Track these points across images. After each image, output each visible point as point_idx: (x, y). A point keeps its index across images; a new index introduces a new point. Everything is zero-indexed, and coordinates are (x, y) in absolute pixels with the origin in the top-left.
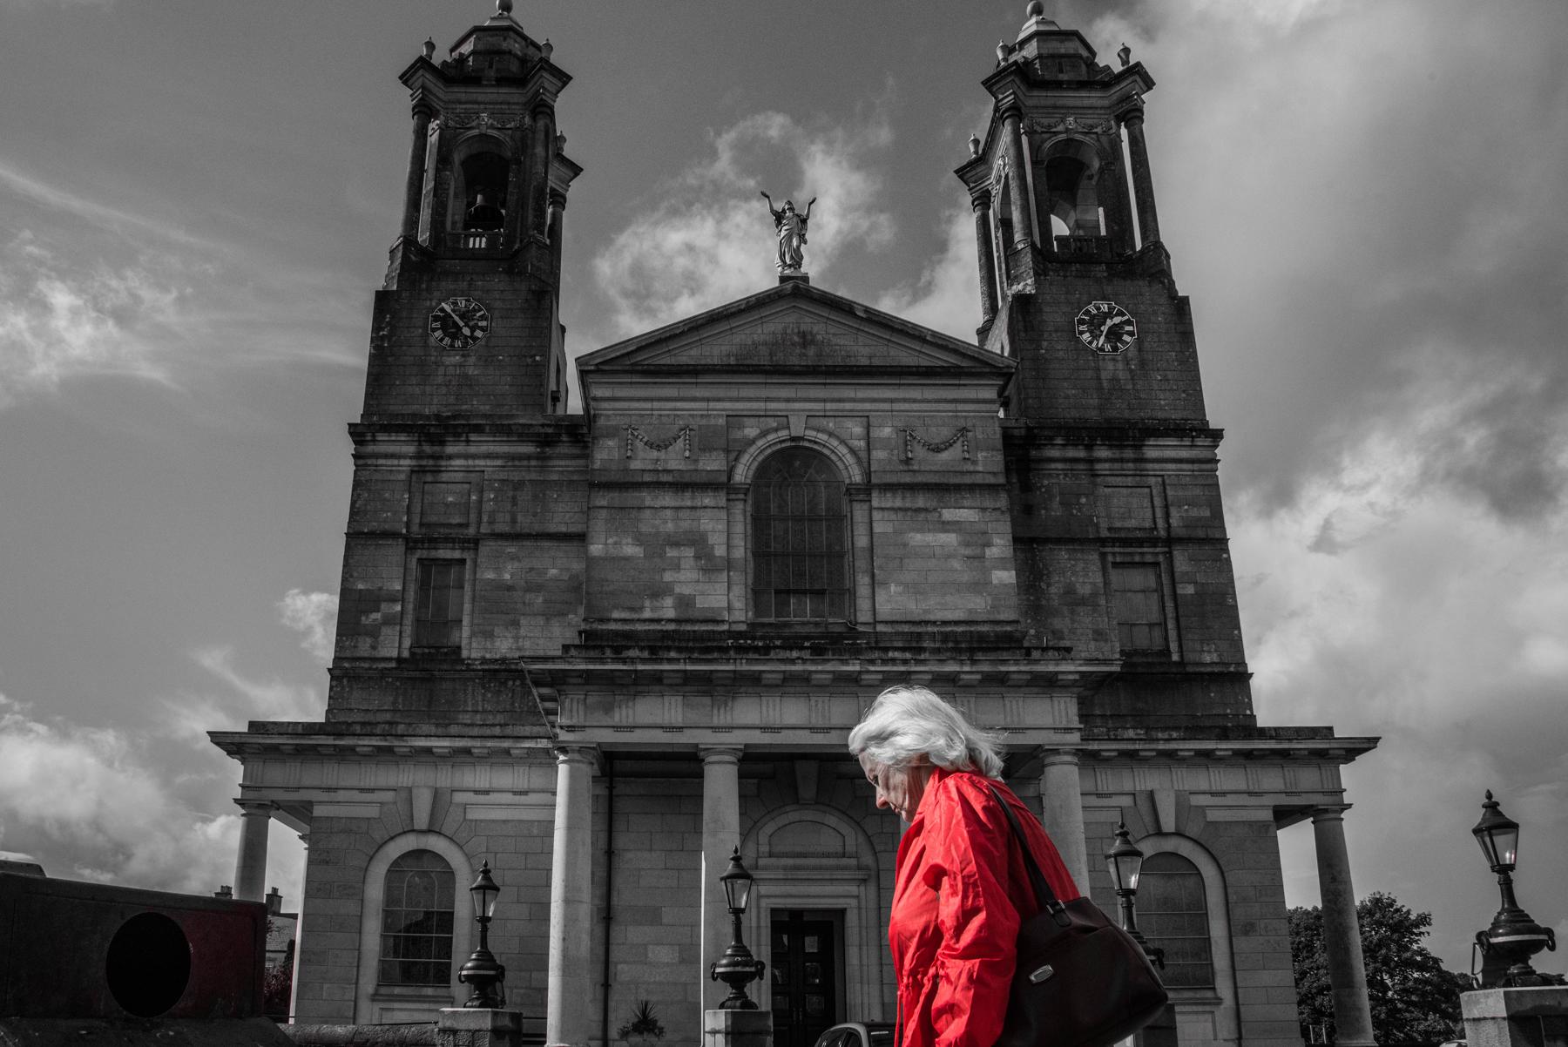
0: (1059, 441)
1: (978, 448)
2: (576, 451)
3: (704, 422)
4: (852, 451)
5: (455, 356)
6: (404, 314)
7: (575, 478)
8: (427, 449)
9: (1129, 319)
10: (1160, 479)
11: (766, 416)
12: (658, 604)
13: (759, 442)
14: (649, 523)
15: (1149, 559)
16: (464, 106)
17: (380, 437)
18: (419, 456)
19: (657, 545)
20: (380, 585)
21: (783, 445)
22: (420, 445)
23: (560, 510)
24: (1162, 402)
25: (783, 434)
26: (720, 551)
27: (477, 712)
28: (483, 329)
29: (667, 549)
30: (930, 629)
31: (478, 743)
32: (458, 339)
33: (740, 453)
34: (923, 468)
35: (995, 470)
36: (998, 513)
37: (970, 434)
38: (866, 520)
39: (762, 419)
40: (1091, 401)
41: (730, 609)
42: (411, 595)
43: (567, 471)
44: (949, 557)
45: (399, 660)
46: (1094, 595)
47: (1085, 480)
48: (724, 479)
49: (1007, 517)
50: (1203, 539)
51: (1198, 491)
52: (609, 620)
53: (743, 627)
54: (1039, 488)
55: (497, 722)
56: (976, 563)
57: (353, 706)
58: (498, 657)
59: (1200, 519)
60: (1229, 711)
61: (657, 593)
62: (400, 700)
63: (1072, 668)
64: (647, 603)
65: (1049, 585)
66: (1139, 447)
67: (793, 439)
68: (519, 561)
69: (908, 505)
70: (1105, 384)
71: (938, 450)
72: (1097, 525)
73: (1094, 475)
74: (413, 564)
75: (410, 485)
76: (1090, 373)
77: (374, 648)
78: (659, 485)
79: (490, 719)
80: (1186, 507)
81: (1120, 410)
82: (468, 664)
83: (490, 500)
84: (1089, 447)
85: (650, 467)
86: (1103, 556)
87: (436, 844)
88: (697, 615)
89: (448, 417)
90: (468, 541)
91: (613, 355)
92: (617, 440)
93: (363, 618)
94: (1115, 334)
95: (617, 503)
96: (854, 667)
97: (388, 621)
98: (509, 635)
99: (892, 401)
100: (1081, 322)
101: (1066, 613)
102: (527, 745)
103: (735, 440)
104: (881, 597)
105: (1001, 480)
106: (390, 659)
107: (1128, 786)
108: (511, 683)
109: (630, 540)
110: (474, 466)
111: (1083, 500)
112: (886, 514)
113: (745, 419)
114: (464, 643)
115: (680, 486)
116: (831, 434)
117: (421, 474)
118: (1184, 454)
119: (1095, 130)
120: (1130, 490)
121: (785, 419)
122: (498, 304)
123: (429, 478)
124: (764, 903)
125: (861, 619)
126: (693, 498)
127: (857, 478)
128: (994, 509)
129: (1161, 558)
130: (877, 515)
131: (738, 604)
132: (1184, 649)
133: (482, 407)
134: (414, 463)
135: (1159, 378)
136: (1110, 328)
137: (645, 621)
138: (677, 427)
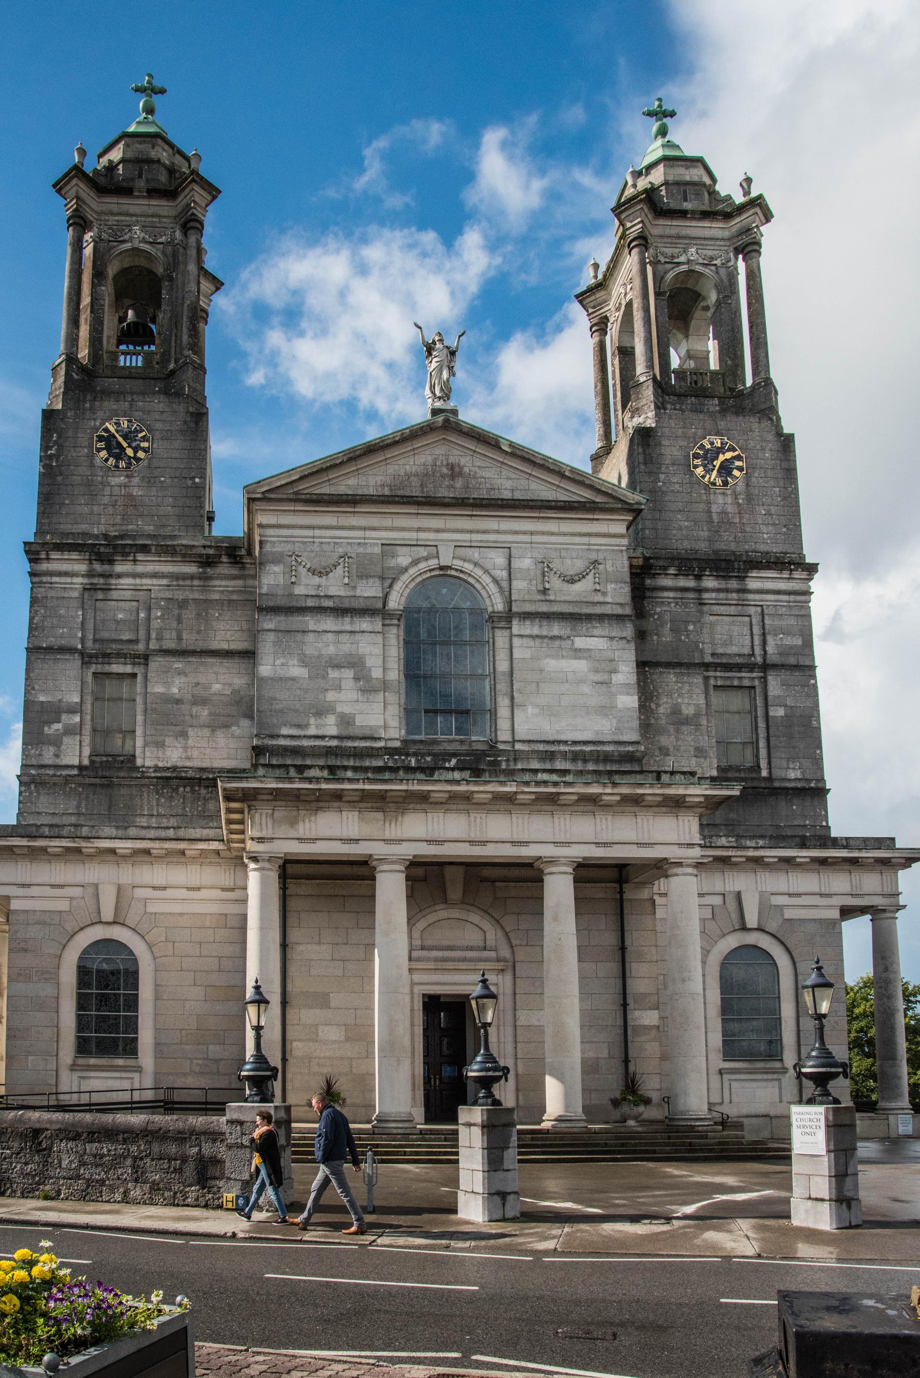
0: (672, 571)
2: (235, 572)
7: (235, 597)
8: (97, 567)
10: (759, 609)
12: (323, 722)
14: (312, 646)
17: (54, 555)
18: (90, 574)
22: (91, 563)
23: (222, 628)
26: (377, 673)
27: (153, 815)
28: (145, 450)
30: (563, 748)
31: (157, 844)
33: (394, 580)
34: (558, 599)
35: (623, 602)
36: (624, 641)
37: (601, 567)
38: (507, 646)
40: (702, 533)
41: (385, 727)
42: (88, 707)
44: (581, 681)
49: (632, 646)
52: (278, 736)
53: (397, 744)
55: (170, 825)
56: (603, 687)
58: (169, 765)
61: (321, 712)
62: (83, 805)
63: (698, 792)
64: (312, 721)
66: (742, 578)
67: (442, 568)
68: (186, 676)
69: (545, 633)
71: (572, 581)
74: (89, 678)
75: (83, 602)
79: (165, 822)
81: (727, 543)
82: (143, 772)
83: (157, 618)
84: (698, 577)
85: (314, 593)
88: (359, 733)
89: (116, 537)
92: (282, 566)
96: (511, 788)
98: (178, 745)
102: (200, 847)
103: (389, 568)
104: (519, 716)
105: (628, 611)
106: (72, 767)
108: (181, 789)
109: (295, 662)
110: (141, 585)
112: (525, 640)
114: (138, 752)
117: (93, 591)
118: (782, 586)
120: (732, 618)
121: (434, 548)
123: (100, 595)
124: (418, 990)
125: (500, 738)
126: (351, 623)
127: (500, 606)
128: (621, 638)
130: (516, 642)
131: (394, 722)
134: (86, 581)
137: (310, 737)
138: (336, 555)
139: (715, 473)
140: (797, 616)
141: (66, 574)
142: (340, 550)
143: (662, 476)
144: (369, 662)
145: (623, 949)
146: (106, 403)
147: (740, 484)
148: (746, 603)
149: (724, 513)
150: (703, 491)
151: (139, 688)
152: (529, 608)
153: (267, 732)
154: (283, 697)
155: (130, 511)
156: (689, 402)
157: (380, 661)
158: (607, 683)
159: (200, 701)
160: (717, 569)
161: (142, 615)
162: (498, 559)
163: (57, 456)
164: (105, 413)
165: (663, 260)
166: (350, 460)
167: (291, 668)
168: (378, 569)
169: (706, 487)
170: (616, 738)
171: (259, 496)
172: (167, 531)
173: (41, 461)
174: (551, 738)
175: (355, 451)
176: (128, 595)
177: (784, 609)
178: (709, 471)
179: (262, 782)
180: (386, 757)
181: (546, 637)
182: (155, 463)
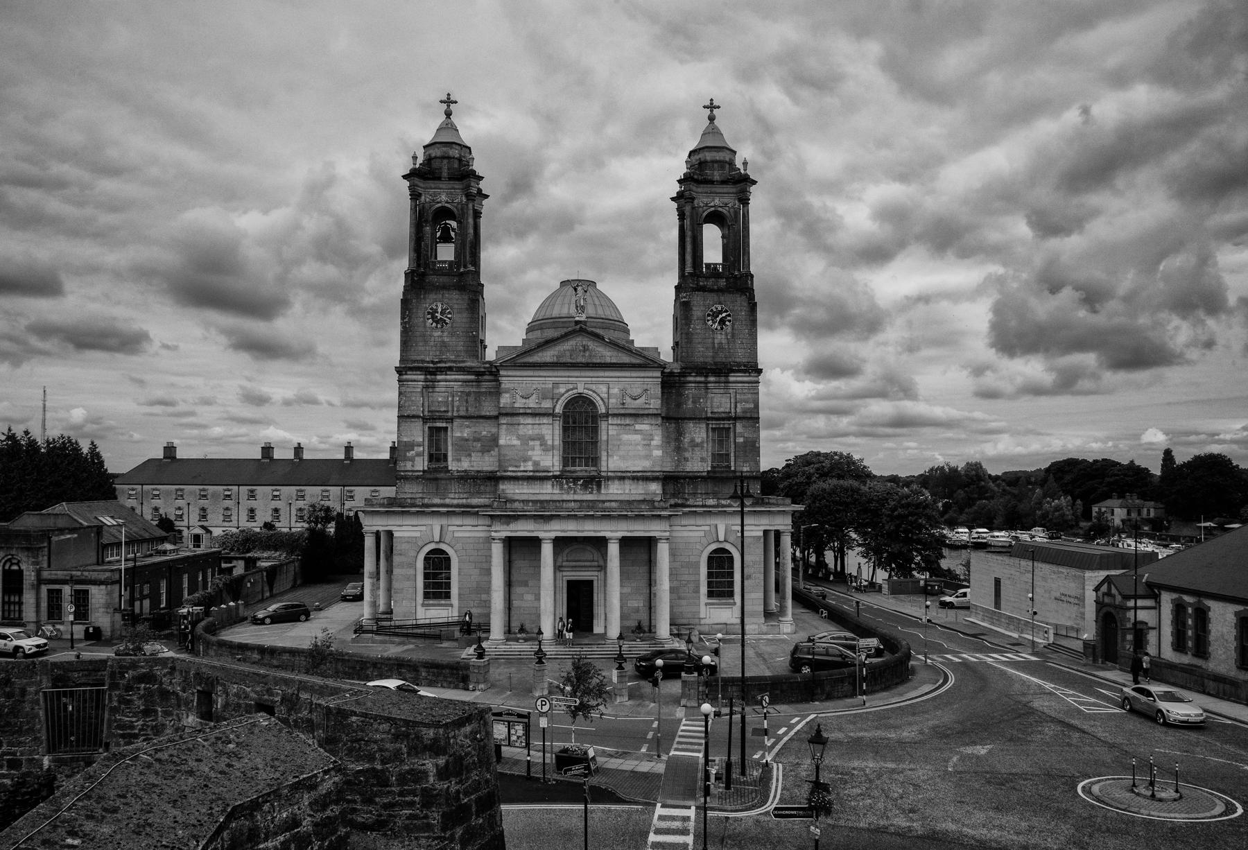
3: (544, 386)
4: (602, 399)
8: (429, 377)
14: (522, 430)
15: (727, 426)
18: (426, 381)
19: (525, 440)
25: (575, 391)
26: (550, 442)
30: (629, 474)
33: (558, 399)
42: (426, 443)
45: (424, 471)
46: (702, 442)
47: (703, 391)
48: (551, 412)
51: (750, 396)
53: (558, 473)
59: (749, 409)
61: (525, 461)
64: (522, 464)
70: (716, 345)
72: (706, 412)
74: (426, 429)
77: (413, 466)
79: (462, 496)
81: (721, 358)
86: (708, 425)
87: (443, 547)
88: (542, 469)
89: (437, 362)
94: (722, 322)
95: (510, 422)
97: (418, 455)
100: (709, 315)
106: (420, 471)
107: (708, 523)
115: (534, 415)
116: (594, 392)
122: (456, 306)
129: (731, 426)
131: (557, 463)
141: (415, 381)
143: (692, 326)
145: (650, 561)
151: (449, 433)
152: (616, 412)
154: (510, 454)
155: (443, 349)
158: (649, 445)
159: (477, 440)
162: (603, 389)
163: (408, 322)
166: (538, 347)
176: (443, 389)
178: (714, 323)
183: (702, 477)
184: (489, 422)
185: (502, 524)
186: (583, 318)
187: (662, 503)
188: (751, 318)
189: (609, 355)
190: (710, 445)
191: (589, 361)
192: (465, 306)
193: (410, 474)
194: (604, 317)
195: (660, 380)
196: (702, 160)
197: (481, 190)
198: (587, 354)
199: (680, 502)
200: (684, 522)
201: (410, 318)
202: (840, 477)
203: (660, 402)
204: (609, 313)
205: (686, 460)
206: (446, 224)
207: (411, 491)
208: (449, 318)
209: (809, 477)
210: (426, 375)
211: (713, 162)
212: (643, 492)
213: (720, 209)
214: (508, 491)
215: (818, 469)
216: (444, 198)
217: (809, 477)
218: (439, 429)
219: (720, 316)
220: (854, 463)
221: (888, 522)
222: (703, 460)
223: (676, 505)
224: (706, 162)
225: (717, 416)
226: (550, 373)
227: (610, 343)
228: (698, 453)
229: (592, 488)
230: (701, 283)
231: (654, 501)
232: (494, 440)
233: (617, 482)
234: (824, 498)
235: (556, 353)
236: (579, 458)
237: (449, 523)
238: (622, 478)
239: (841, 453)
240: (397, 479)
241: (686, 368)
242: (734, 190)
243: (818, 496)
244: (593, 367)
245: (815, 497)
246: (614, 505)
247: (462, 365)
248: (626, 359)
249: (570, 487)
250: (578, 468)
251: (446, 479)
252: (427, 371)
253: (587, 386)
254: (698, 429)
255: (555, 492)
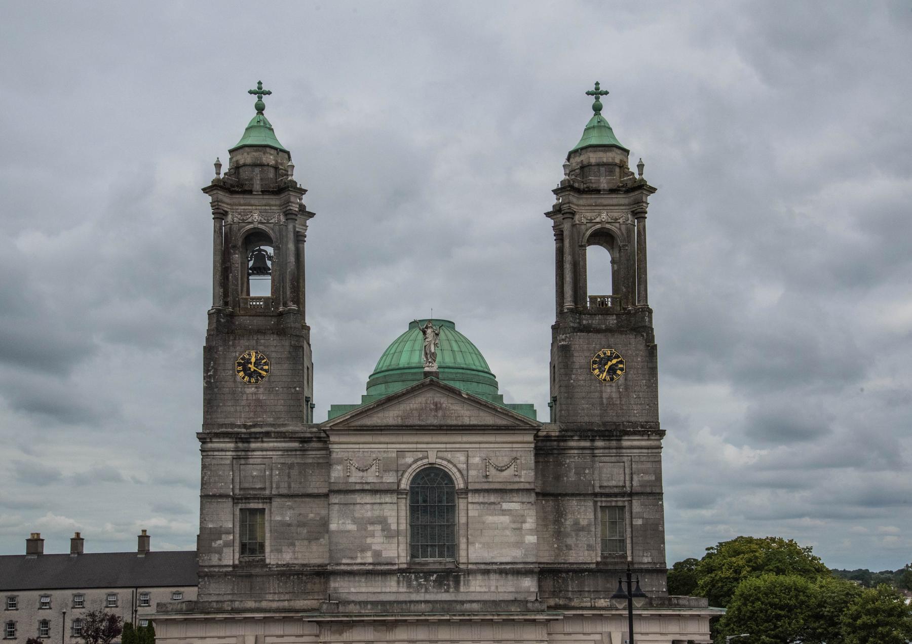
1: (522, 469)
3: (385, 455)
4: (459, 471)
5: (251, 388)
6: (221, 361)
7: (321, 461)
8: (240, 445)
9: (621, 360)
10: (630, 458)
11: (416, 451)
13: (412, 464)
14: (359, 512)
15: (620, 504)
16: (243, 207)
18: (236, 450)
19: (363, 524)
20: (221, 525)
21: (426, 467)
23: (314, 480)
24: (635, 412)
25: (425, 461)
26: (394, 527)
29: (368, 526)
30: (495, 567)
32: (252, 377)
33: (404, 472)
34: (494, 481)
36: (530, 505)
37: (518, 461)
38: (466, 508)
39: (415, 453)
40: (596, 411)
41: (398, 557)
43: (316, 457)
45: (234, 566)
46: (589, 525)
47: (588, 459)
48: (396, 487)
50: (650, 493)
51: (649, 465)
52: (341, 564)
53: (405, 566)
54: (564, 465)
55: (286, 599)
56: (518, 532)
57: (211, 592)
58: (285, 563)
60: (654, 589)
61: (363, 551)
62: (236, 589)
64: (359, 555)
65: (566, 520)
68: (294, 509)
69: (486, 501)
70: (605, 401)
72: (593, 486)
73: (594, 456)
74: (238, 512)
75: (233, 466)
76: (597, 394)
78: (363, 491)
80: (642, 475)
82: (270, 568)
83: (276, 475)
85: (359, 481)
86: (595, 502)
88: (383, 560)
89: (251, 427)
90: (266, 498)
91: (339, 421)
92: (342, 465)
93: (213, 544)
94: (612, 370)
95: (343, 501)
97: (227, 545)
98: (290, 551)
99: (480, 443)
100: (595, 362)
101: (574, 535)
107: (599, 629)
108: (292, 577)
109: (350, 522)
110: (267, 455)
111: (587, 471)
112: (475, 505)
113: (406, 453)
115: (374, 492)
116: (449, 461)
117: (238, 460)
118: (644, 443)
119: (619, 221)
120: (613, 464)
121: (426, 453)
122: (274, 355)
123: (243, 462)
125: (461, 561)
126: (380, 498)
129: (626, 504)
130: (470, 506)
131: (403, 554)
132: (634, 555)
133: (268, 419)
134: (234, 454)
135: (635, 396)
136: (610, 367)
137: (358, 564)
139: (605, 373)
140: (653, 462)
141: (222, 450)
142: (374, 456)
143: (573, 376)
144: (390, 521)
146: (242, 341)
147: (621, 379)
148: (621, 455)
149: (610, 398)
150: (598, 385)
151: (267, 517)
152: (478, 486)
153: (334, 562)
155: (259, 409)
156: (597, 318)
157: (395, 520)
158: (520, 529)
159: (302, 524)
160: (603, 436)
161: (267, 473)
163: (214, 376)
164: (241, 347)
165: (584, 221)
166: (378, 406)
167: (347, 525)
168: (394, 467)
169: (600, 382)
170: (524, 560)
171: (328, 428)
172: (281, 421)
173: (204, 379)
174: (488, 561)
175: (381, 401)
176: (259, 461)
177: (645, 458)
178: (602, 372)
179: (323, 618)
180: (399, 574)
181: (487, 503)
182: (272, 379)
183: (590, 571)
184: (317, 500)
185: (334, 633)
186: (434, 368)
187: (537, 605)
188: (650, 365)
189: (467, 415)
190: (599, 529)
191: (442, 423)
192: (286, 355)
193: (216, 570)
194: (464, 366)
195: (533, 445)
196: (585, 163)
197: (305, 207)
198: (440, 413)
199: (561, 602)
200: (568, 629)
201: (216, 370)
202: (779, 571)
203: (532, 473)
204: (471, 361)
205: (569, 548)
206: (260, 250)
207: (217, 592)
208: (266, 371)
209: (737, 571)
210: (236, 442)
211: (598, 165)
212: (513, 590)
213: (608, 226)
214: (341, 590)
215: (750, 561)
216: (256, 217)
217: (737, 571)
218: (253, 512)
219: (610, 363)
220: (799, 553)
221: (849, 634)
222: (590, 547)
223: (557, 607)
224: (589, 165)
225: (607, 491)
226: (393, 439)
227: (469, 399)
228: (584, 539)
229: (448, 585)
230: (584, 322)
231: (527, 602)
232: (324, 524)
233: (479, 577)
234: (758, 599)
235: (400, 413)
236: (431, 546)
237: (267, 633)
238: (486, 572)
239: (781, 540)
240: (200, 577)
241: (566, 431)
242: (626, 201)
243: (751, 595)
244: (447, 430)
245: (746, 598)
246: (475, 606)
247: (283, 429)
248: (488, 419)
249: (420, 584)
250: (430, 560)
251: (262, 576)
252: (238, 438)
253: (440, 454)
254: (583, 508)
255: (401, 590)
